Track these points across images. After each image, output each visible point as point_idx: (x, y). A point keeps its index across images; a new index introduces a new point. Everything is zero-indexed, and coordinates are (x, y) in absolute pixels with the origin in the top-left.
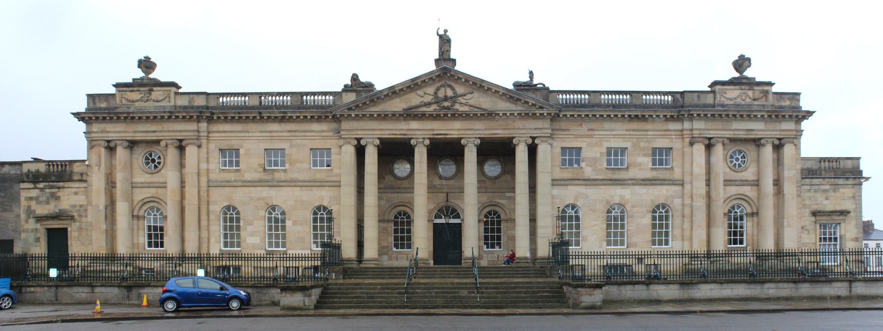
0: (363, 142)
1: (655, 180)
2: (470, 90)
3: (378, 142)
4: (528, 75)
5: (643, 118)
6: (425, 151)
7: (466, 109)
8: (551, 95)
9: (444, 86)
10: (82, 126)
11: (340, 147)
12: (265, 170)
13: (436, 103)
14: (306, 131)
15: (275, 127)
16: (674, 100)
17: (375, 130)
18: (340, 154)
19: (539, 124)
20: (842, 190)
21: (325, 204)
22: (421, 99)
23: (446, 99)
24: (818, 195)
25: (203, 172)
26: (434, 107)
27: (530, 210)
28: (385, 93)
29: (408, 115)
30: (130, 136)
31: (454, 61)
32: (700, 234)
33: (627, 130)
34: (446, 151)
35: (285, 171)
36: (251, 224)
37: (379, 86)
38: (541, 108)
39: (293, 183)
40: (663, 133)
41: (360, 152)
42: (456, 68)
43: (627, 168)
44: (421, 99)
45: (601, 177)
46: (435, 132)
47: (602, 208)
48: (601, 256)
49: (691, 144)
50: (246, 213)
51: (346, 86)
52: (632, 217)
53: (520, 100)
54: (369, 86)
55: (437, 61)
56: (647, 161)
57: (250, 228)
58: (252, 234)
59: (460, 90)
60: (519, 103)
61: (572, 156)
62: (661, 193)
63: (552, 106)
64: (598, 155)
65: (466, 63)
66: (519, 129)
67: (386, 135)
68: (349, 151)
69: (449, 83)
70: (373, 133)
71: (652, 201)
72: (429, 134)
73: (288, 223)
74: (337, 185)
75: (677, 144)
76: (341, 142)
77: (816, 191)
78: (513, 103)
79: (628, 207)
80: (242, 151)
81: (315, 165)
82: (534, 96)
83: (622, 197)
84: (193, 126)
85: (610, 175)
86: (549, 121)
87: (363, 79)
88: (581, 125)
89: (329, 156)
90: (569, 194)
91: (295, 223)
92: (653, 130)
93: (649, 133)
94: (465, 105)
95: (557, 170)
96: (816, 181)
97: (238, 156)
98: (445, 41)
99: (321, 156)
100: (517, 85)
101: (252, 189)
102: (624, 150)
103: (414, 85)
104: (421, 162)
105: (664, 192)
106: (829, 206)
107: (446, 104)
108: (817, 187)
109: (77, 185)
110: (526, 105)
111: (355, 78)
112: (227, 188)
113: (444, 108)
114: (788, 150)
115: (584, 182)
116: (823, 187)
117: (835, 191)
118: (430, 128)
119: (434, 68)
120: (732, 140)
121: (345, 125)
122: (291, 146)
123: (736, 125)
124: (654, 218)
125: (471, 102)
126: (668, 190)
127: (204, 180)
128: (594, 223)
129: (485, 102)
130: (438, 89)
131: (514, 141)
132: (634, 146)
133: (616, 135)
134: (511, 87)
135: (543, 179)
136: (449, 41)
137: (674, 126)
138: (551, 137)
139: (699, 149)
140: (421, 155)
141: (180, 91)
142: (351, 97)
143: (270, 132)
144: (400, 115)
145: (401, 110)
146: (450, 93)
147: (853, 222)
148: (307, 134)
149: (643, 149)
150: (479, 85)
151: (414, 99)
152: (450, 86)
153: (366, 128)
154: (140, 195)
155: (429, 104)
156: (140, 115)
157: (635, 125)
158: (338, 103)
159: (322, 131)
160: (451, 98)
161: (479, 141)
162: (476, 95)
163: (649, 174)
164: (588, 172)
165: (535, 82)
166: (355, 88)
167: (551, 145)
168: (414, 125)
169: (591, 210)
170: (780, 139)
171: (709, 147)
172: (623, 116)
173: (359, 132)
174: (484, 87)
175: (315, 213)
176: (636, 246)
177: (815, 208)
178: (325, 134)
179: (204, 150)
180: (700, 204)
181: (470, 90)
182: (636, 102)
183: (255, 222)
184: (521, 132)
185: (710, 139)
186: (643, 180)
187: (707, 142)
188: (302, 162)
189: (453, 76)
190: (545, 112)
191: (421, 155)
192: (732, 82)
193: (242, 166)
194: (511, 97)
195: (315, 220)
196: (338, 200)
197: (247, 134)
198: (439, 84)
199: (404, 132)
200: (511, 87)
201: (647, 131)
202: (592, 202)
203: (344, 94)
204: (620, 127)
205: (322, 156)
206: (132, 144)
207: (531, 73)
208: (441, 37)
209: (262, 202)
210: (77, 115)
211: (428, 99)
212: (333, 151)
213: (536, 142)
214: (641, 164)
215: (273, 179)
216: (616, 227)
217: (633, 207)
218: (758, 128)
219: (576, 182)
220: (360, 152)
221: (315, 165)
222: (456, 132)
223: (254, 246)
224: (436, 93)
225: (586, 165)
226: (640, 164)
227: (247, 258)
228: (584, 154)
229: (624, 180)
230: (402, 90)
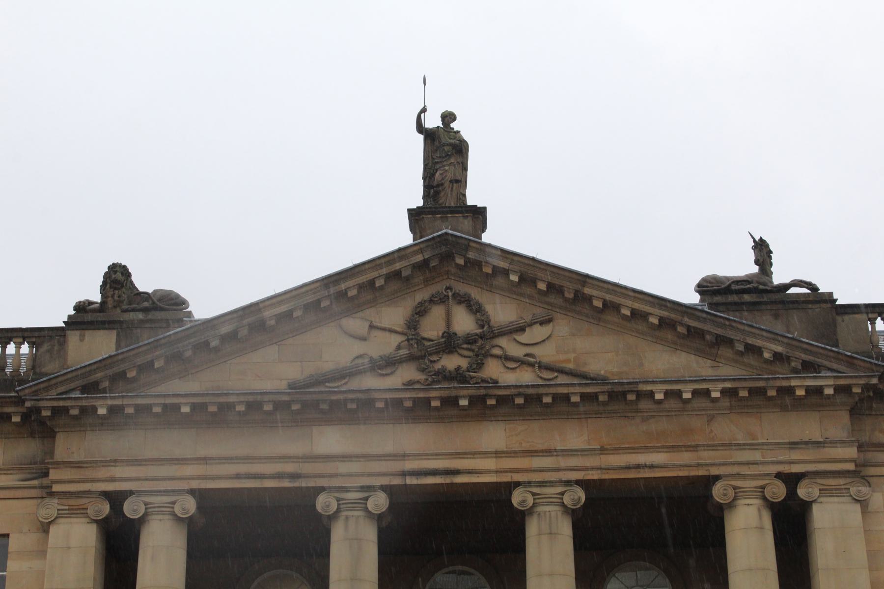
0: (131, 509)
2: (540, 312)
3: (190, 505)
4: (751, 256)
6: (370, 535)
7: (526, 377)
8: (845, 322)
9: (439, 299)
11: (45, 528)
13: (411, 358)
18: (42, 553)
19: (807, 426)
22: (358, 348)
23: (450, 343)
28: (225, 329)
29: (305, 405)
31: (479, 214)
37: (204, 306)
38: (809, 367)
42: (486, 238)
44: (358, 348)
51: (81, 307)
53: (730, 342)
55: (415, 215)
59: (502, 311)
60: (725, 352)
63: (850, 362)
65: (520, 217)
66: (728, 446)
67: (223, 478)
69: (461, 288)
72: (386, 473)
76: (52, 507)
78: (701, 353)
82: (779, 328)
86: (845, 417)
94: (522, 362)
98: (444, 150)
100: (709, 288)
104: (354, 579)
107: (451, 362)
110: (751, 360)
111: (117, 278)
113: (445, 376)
118: (389, 448)
119: (401, 236)
125: (546, 353)
129: (602, 354)
130: (421, 311)
131: (718, 492)
134: (693, 298)
136: (460, 149)
138: (859, 473)
144: (279, 406)
145: (283, 385)
146: (464, 323)
152: (466, 301)
153: (148, 454)
158: (51, 367)
160: (470, 340)
162: (562, 327)
165: (779, 277)
166: (117, 315)
167: (863, 503)
168: (330, 440)
174: (589, 299)
181: (540, 312)
184: (743, 458)
189: (478, 264)
190: (827, 383)
194: (694, 334)
198: (422, 295)
199: (290, 468)
200: (693, 298)
203: (73, 337)
207: (762, 250)
208: (430, 136)
212: (14, 543)
213: (802, 492)
222: (490, 464)
224: (413, 324)
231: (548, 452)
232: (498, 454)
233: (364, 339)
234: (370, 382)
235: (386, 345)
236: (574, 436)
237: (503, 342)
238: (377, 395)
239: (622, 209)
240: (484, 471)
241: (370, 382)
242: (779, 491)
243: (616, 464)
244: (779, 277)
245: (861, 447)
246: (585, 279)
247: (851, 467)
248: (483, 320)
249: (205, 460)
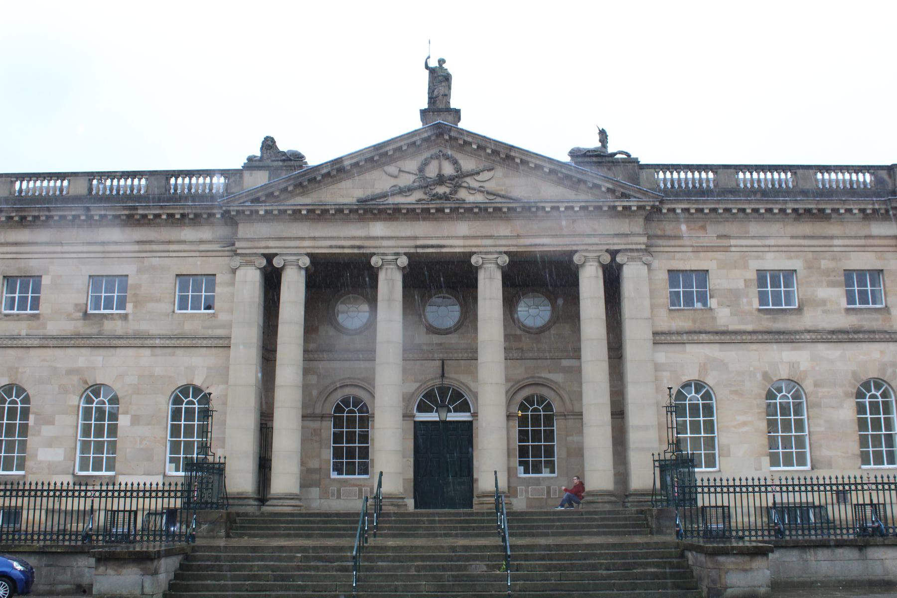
0: (277, 262)
1: (857, 332)
2: (487, 164)
3: (306, 261)
4: (598, 137)
5: (821, 215)
6: (398, 278)
7: (479, 198)
8: (644, 174)
11: (234, 271)
12: (86, 315)
13: (420, 187)
14: (169, 242)
16: (878, 181)
17: (302, 239)
18: (232, 284)
19: (624, 226)
21: (198, 382)
22: (393, 182)
23: (441, 180)
27: (613, 393)
28: (325, 171)
29: (366, 211)
31: (457, 112)
33: (792, 237)
34: (440, 279)
35: (125, 317)
36: (51, 422)
37: (313, 159)
38: (624, 196)
40: (862, 242)
41: (272, 280)
42: (461, 125)
43: (800, 310)
44: (393, 182)
45: (749, 327)
46: (419, 242)
47: (756, 388)
48: (762, 487)
51: (250, 159)
52: (818, 405)
53: (585, 182)
54: (296, 158)
55: (423, 113)
56: (837, 295)
57: (47, 431)
58: (50, 443)
59: (468, 164)
60: (582, 186)
61: (689, 287)
62: (870, 358)
63: (645, 193)
64: (741, 285)
66: (580, 235)
67: (323, 247)
68: (250, 280)
70: (297, 245)
71: (854, 374)
72: (408, 246)
73: (123, 421)
74: (224, 344)
76: (237, 261)
78: (571, 187)
79: (808, 385)
80: (46, 281)
81: (183, 305)
82: (610, 175)
83: (793, 365)
85: (767, 323)
86: (641, 221)
87: (283, 146)
88: (703, 228)
89: (211, 287)
90: (689, 362)
91: (136, 420)
92: (842, 237)
93: (836, 242)
95: (663, 313)
97: (37, 289)
98: (439, 78)
99: (195, 289)
100: (575, 154)
101: (58, 352)
102: (790, 274)
103: (379, 156)
104: (390, 300)
105: (876, 355)
107: (441, 190)
110: (595, 191)
111: (269, 144)
112: (11, 352)
113: (437, 197)
115: (717, 338)
119: (416, 124)
121: (245, 230)
122: (140, 271)
124: (861, 409)
125: (490, 186)
126: (881, 352)
128: (741, 418)
130: (426, 163)
132: (809, 267)
133: (774, 247)
134: (566, 159)
135: (636, 333)
136: (447, 78)
138: (648, 250)
140: (390, 284)
143: (103, 243)
144: (351, 211)
145: (354, 201)
146: (448, 170)
148: (172, 247)
149: (827, 273)
150: (504, 156)
152: (447, 158)
153: (285, 235)
157: (806, 228)
158: (235, 190)
159: (202, 242)
160: (451, 178)
161: (506, 259)
162: (499, 172)
164: (724, 317)
165: (611, 149)
166: (268, 162)
167: (649, 265)
168: (378, 229)
169: (735, 392)
172: (782, 211)
173: (271, 244)
174: (513, 158)
175: (177, 401)
176: (829, 465)
178: (203, 247)
181: (487, 164)
182: (803, 185)
183: (58, 418)
186: (833, 332)
188: (158, 300)
189: (456, 139)
190: (633, 204)
191: (390, 284)
193: (44, 308)
194: (567, 177)
195: (176, 415)
196: (223, 373)
197: (59, 249)
198: (427, 155)
199: (357, 243)
200: (566, 159)
201: (832, 238)
202: (738, 377)
203: (246, 174)
204: (779, 232)
205: (197, 289)
207: (603, 134)
208: (432, 71)
209: (75, 379)
211: (406, 180)
212: (219, 279)
215: (100, 333)
216: (786, 426)
217: (816, 385)
219: (703, 337)
220: (272, 280)
221: (183, 305)
222: (460, 242)
223: (52, 468)
224: (421, 170)
225: (720, 304)
226: (823, 302)
227: (36, 492)
228: (716, 281)
229: (796, 332)
230: (356, 164)
231: (490, 237)
232: (465, 237)
233: (396, 177)
234: (399, 199)
237: (468, 179)
238: (402, 206)
239: (530, 110)
242: (607, 259)
245: (649, 237)
246: (512, 148)
247: (643, 247)
248: (458, 168)
249: (314, 238)
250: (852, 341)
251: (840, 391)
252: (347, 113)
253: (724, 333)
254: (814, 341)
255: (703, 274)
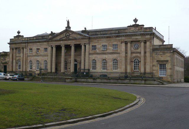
0: (52, 46)
6: (64, 47)
10: (9, 45)
15: (38, 44)
16: (119, 32)
20: (166, 54)
23: (67, 36)
24: (159, 56)
25: (26, 54)
26: (65, 38)
30: (15, 47)
32: (123, 67)
35: (40, 53)
39: (41, 55)
43: (107, 50)
47: (100, 60)
49: (122, 43)
50: (33, 62)
57: (34, 65)
61: (94, 47)
62: (115, 56)
72: (65, 44)
75: (119, 43)
77: (158, 55)
79: (107, 60)
83: (105, 57)
84: (25, 44)
85: (102, 52)
87: (53, 32)
90: (93, 57)
96: (159, 52)
98: (68, 22)
99: (46, 49)
102: (106, 45)
106: (162, 59)
107: (68, 37)
108: (158, 54)
109: (8, 57)
111: (52, 32)
114: (148, 43)
116: (161, 53)
117: (164, 54)
120: (132, 41)
121: (50, 43)
123: (133, 37)
124: (114, 63)
127: (26, 55)
130: (66, 34)
131: (81, 45)
132: (108, 44)
133: (104, 42)
135: (87, 53)
137: (118, 38)
139: (123, 45)
141: (24, 37)
142: (50, 37)
147: (170, 64)
151: (62, 36)
154: (17, 58)
155: (64, 37)
156: (18, 43)
157: (108, 39)
160: (68, 35)
163: (111, 51)
164: (98, 51)
168: (62, 42)
170: (145, 41)
171: (126, 43)
177: (158, 59)
179: (27, 49)
180: (124, 59)
184: (82, 42)
185: (126, 42)
186: (110, 53)
187: (125, 42)
192: (133, 26)
196: (48, 59)
204: (104, 40)
206: (16, 48)
207: (85, 28)
210: (8, 43)
211: (64, 36)
214: (111, 49)
218: (139, 38)
220: (52, 48)
235: (64, 36)
236: (74, 41)
239: (76, 27)
240: (69, 44)
241: (64, 38)
242: (84, 44)
243: (76, 43)
244: (87, 29)
250: (112, 54)
251: (111, 60)
252: (59, 28)
253: (97, 53)
254: (108, 54)
255: (96, 46)
